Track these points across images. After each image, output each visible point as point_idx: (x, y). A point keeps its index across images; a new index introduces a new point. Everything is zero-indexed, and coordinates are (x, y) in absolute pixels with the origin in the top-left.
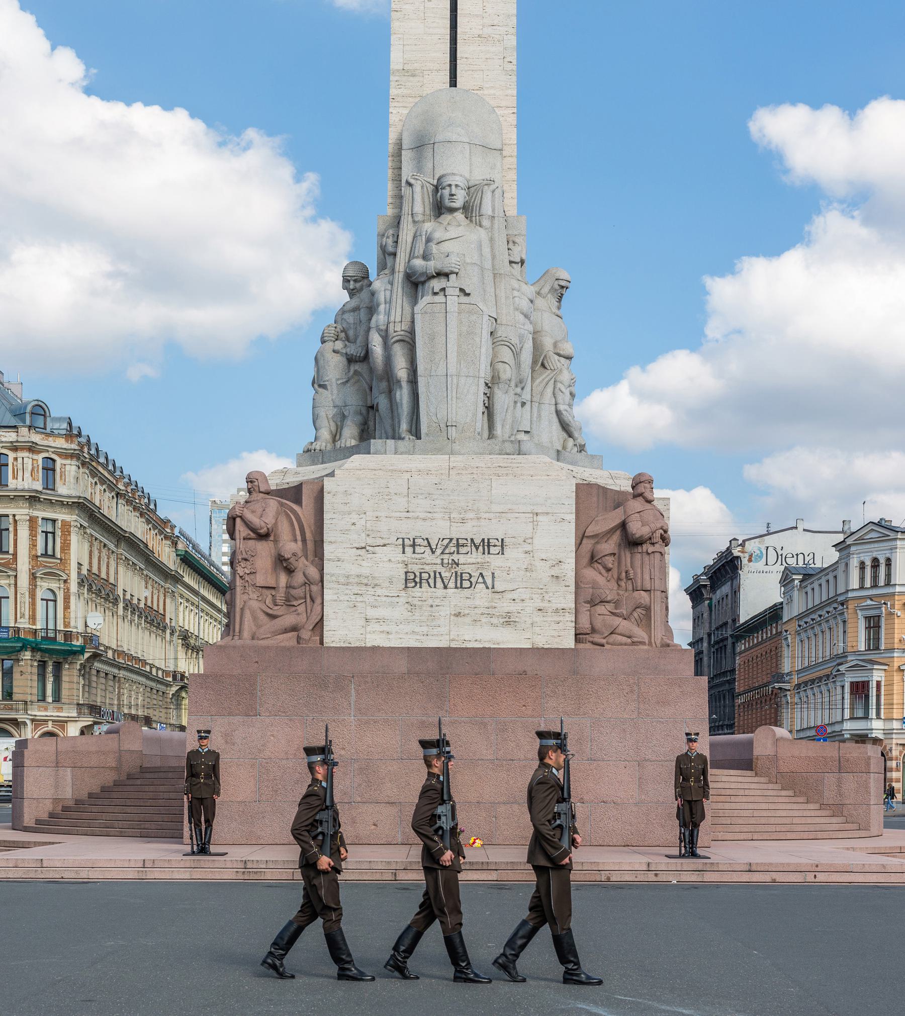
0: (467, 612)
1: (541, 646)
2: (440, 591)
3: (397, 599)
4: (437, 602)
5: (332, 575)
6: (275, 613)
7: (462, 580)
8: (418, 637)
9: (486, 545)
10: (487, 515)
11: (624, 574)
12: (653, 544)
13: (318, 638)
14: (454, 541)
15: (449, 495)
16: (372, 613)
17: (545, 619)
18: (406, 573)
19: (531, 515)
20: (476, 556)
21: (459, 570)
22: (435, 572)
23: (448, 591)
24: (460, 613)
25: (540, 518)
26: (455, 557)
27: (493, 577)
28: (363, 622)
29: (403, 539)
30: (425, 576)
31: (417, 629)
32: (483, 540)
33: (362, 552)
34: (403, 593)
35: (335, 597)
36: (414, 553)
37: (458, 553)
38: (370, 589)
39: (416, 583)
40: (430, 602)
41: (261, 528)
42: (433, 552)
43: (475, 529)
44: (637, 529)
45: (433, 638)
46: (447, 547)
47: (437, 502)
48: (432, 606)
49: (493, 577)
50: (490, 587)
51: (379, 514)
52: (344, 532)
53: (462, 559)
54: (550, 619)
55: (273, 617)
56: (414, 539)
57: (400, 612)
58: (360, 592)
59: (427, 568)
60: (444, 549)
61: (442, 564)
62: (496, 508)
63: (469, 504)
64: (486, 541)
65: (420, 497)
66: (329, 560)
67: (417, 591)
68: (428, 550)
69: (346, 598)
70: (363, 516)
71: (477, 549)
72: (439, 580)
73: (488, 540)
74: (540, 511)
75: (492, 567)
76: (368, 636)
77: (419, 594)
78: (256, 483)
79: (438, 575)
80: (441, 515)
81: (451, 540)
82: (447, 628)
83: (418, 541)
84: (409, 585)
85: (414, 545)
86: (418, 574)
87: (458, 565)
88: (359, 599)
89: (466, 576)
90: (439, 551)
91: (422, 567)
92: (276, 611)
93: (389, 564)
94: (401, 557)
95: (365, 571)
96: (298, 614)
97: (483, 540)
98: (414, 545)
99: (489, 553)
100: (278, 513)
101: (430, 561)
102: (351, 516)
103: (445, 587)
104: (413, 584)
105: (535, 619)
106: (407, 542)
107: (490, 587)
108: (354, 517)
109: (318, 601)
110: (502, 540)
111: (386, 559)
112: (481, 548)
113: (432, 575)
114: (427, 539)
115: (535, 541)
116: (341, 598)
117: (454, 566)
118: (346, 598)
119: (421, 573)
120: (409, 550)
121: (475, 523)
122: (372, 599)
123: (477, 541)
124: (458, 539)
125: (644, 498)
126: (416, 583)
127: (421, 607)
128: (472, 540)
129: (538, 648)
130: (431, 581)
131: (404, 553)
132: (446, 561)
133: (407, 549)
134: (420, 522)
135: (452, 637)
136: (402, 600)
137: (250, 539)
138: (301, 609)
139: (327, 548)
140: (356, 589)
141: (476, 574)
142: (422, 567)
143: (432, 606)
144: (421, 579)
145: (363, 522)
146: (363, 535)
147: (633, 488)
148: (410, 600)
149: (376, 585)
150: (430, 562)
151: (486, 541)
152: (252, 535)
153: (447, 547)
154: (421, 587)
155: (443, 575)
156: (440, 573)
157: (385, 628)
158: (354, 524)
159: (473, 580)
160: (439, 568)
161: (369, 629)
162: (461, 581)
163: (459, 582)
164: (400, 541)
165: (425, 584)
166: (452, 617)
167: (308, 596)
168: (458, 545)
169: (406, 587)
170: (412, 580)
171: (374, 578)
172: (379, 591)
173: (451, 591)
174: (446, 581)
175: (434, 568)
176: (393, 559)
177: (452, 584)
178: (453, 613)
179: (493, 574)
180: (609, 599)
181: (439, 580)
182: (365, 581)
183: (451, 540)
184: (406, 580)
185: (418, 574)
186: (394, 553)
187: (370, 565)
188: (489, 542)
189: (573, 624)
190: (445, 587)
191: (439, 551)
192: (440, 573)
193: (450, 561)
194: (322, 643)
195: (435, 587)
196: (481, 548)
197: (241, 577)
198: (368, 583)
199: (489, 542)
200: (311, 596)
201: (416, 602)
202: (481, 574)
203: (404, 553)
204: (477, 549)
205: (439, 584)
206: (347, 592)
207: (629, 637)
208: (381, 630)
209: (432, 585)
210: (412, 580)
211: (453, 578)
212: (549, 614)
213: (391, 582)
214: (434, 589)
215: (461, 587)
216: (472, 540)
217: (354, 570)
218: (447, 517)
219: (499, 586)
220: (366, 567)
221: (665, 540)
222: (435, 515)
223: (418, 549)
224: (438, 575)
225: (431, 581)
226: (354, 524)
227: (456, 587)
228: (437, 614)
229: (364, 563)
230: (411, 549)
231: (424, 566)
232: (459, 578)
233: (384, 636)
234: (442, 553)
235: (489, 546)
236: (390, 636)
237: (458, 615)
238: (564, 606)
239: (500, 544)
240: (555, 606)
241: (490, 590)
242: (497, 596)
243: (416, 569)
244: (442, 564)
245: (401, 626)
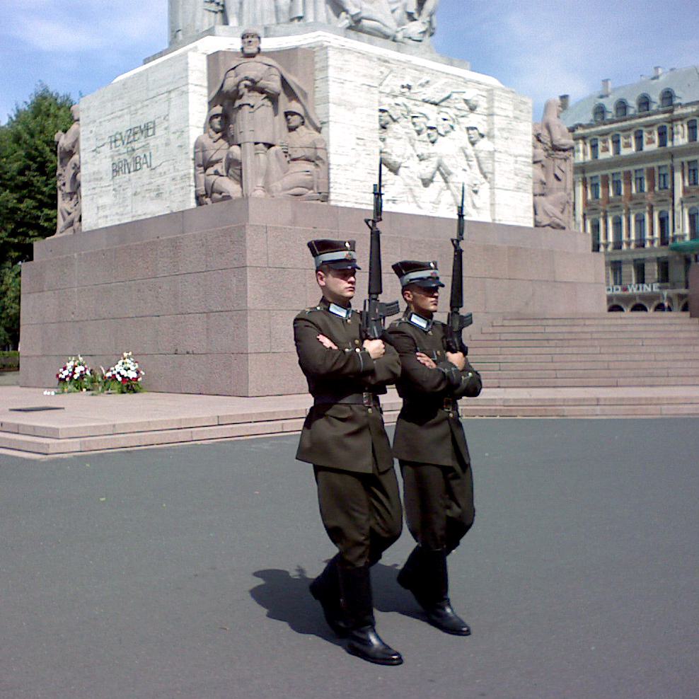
2: (127, 176)
3: (109, 188)
8: (118, 217)
21: (134, 155)
25: (173, 95)
27: (150, 156)
34: (112, 183)
42: (123, 143)
49: (150, 156)
52: (88, 139)
59: (122, 157)
74: (172, 88)
81: (131, 130)
87: (134, 150)
90: (126, 142)
98: (115, 141)
115: (170, 118)
135: (134, 213)
141: (142, 156)
142: (118, 157)
149: (101, 178)
150: (121, 152)
153: (129, 137)
165: (120, 172)
190: (129, 172)
191: (126, 142)
205: (127, 171)
207: (221, 193)
210: (116, 171)
219: (153, 166)
225: (123, 168)
229: (96, 163)
234: (128, 143)
237: (135, 194)
241: (149, 169)
242: (153, 172)
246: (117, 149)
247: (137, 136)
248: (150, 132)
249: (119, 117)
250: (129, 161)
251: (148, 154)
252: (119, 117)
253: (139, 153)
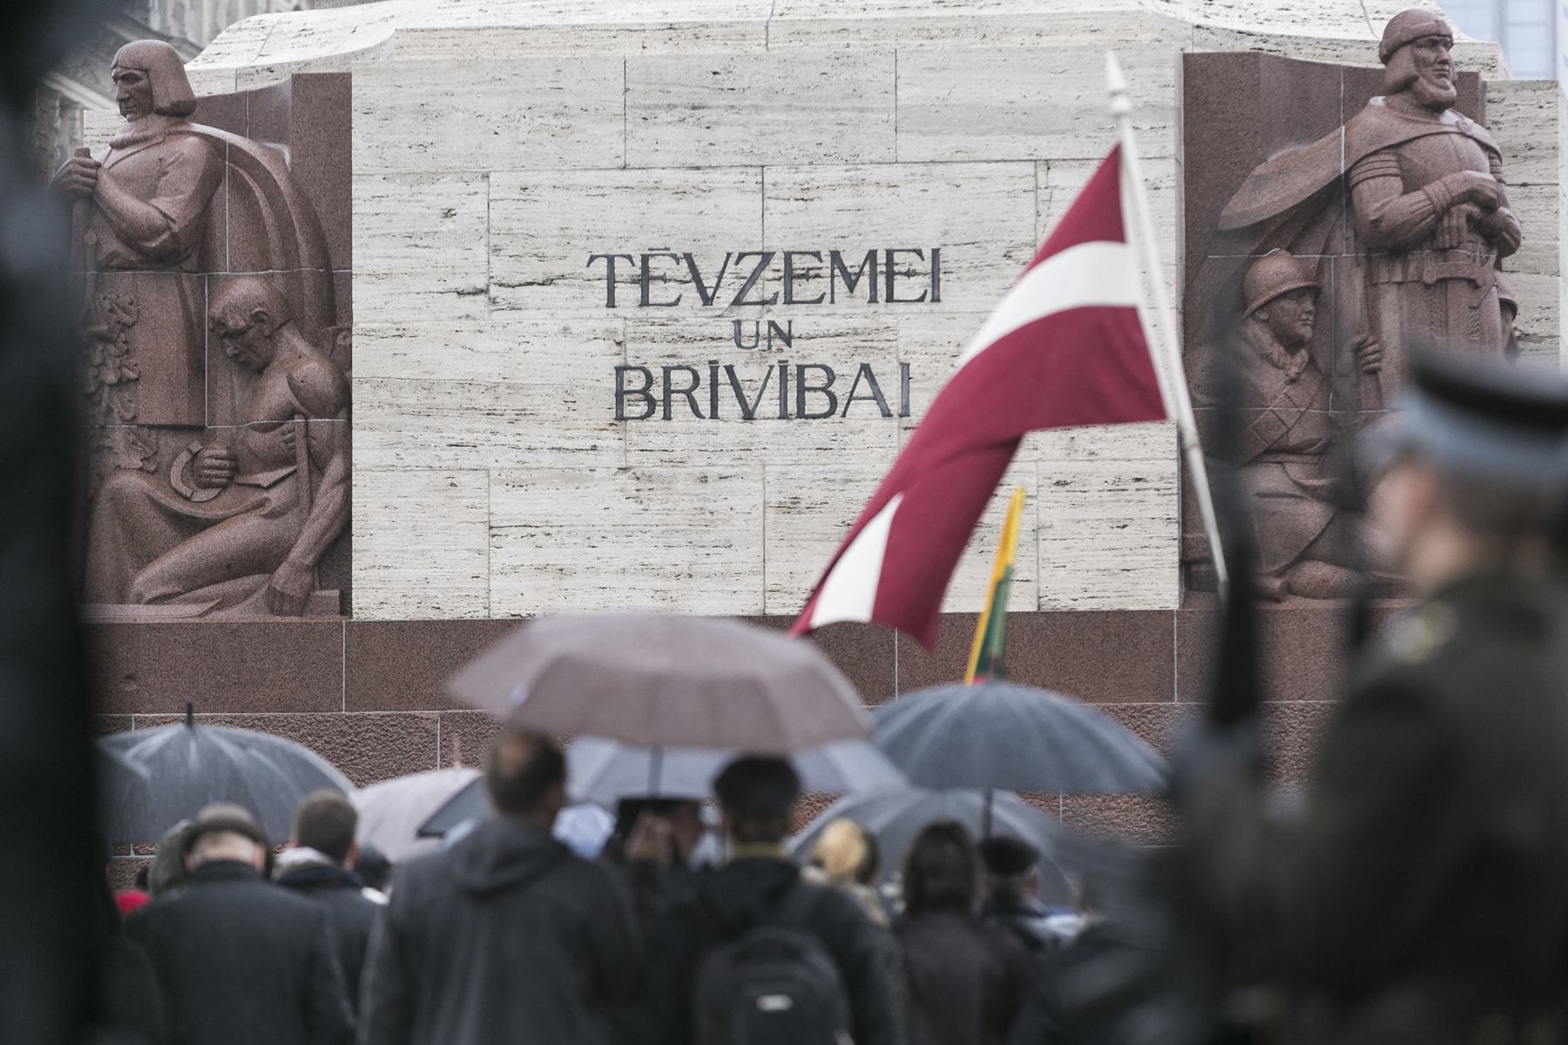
0: (818, 495)
1: (1064, 603)
2: (730, 427)
3: (590, 459)
4: (722, 465)
5: (382, 383)
6: (199, 512)
7: (802, 389)
8: (659, 584)
10: (883, 173)
11: (1347, 357)
12: (1443, 252)
13: (336, 593)
14: (778, 263)
15: (757, 108)
16: (507, 505)
17: (1079, 513)
18: (620, 370)
19: (1030, 168)
20: (851, 310)
22: (714, 366)
23: (757, 426)
24: (796, 500)
26: (780, 314)
27: (906, 378)
28: (479, 538)
29: (611, 260)
30: (681, 379)
31: (658, 557)
32: (872, 255)
33: (478, 304)
34: (610, 440)
35: (389, 457)
36: (644, 303)
37: (789, 301)
38: (502, 426)
39: (652, 403)
40: (699, 465)
41: (155, 232)
42: (707, 301)
43: (846, 219)
44: (1384, 199)
45: (709, 585)
46: (753, 279)
47: (719, 133)
48: (704, 479)
49: (906, 378)
50: (895, 409)
51: (528, 178)
53: (802, 320)
54: (1096, 513)
55: (190, 526)
56: (645, 259)
57: (603, 499)
58: (469, 438)
59: (688, 353)
60: (743, 291)
61: (738, 338)
62: (910, 147)
63: (825, 139)
64: (882, 258)
65: (665, 116)
66: (367, 334)
67: (654, 432)
68: (691, 293)
69: (425, 458)
70: (481, 186)
71: (852, 287)
72: (726, 391)
73: (890, 253)
75: (902, 344)
76: (496, 584)
77: (660, 441)
78: (142, 84)
79: (723, 377)
80: (734, 176)
81: (767, 257)
82: (758, 550)
83: (659, 265)
84: (628, 411)
85: (644, 279)
86: (657, 373)
87: (788, 339)
88: (468, 459)
89: (815, 378)
90: (726, 296)
91: (668, 348)
92: (203, 503)
93: (568, 342)
94: (601, 320)
95: (485, 369)
96: (272, 515)
97: (872, 255)
98: (644, 279)
99: (890, 298)
100: (210, 180)
102: (438, 187)
103: (749, 416)
104: (643, 408)
105: (1048, 516)
106: (622, 267)
107: (895, 409)
108: (449, 191)
109: (335, 468)
110: (936, 252)
111: (552, 326)
112: (864, 282)
113: (705, 374)
114: (688, 257)
116: (409, 460)
117: (778, 343)
118: (425, 458)
119: (667, 371)
120: (628, 294)
121: (846, 199)
122: (508, 459)
123: (853, 260)
124: (788, 256)
125: (1418, 95)
126: (652, 403)
127: (668, 483)
128: (835, 256)
129: (1053, 616)
131: (611, 303)
132: (748, 329)
133: (622, 291)
134: (665, 203)
135: (770, 582)
136: (609, 459)
137: (121, 268)
139: (364, 298)
140: (457, 429)
141: (846, 370)
142: (668, 348)
143: (704, 479)
144: (668, 392)
145: (477, 206)
146: (481, 251)
147: (1385, 59)
148: (633, 459)
149: (522, 413)
150: (698, 331)
151: (882, 258)
153: (753, 279)
154: (667, 417)
155: (741, 374)
156: (730, 370)
157: (552, 554)
158: (448, 214)
159: (840, 389)
160: (727, 353)
161: (499, 559)
163: (792, 396)
164: (601, 267)
165: (680, 407)
166: (771, 514)
167: (302, 453)
168: (789, 276)
169: (621, 418)
171: (514, 388)
172: (533, 434)
173: (766, 427)
174: (750, 395)
175: (710, 351)
176: (576, 327)
177: (769, 406)
178: (774, 500)
179: (905, 367)
180: (1294, 439)
181: (726, 391)
182: (486, 401)
183: (767, 257)
184: (620, 394)
185: (657, 373)
186: (583, 306)
187: (497, 346)
188: (890, 261)
189: (1175, 530)
190: (749, 416)
191: (726, 296)
192: (730, 370)
193: (764, 329)
195: (714, 416)
196: (864, 282)
198: (501, 404)
199: (890, 261)
200: (310, 455)
201: (650, 464)
202: (865, 368)
203: (611, 303)
204: (852, 287)
205: (729, 404)
206: (427, 437)
208: (541, 562)
209: (705, 408)
210: (641, 395)
211: (774, 382)
212: (1093, 496)
213: (570, 403)
214: (709, 423)
215: (801, 414)
216: (835, 256)
217: (452, 366)
218: (752, 178)
220: (483, 351)
221: (1498, 237)
222: (714, 176)
223: (657, 292)
224: (723, 377)
225: (702, 396)
226: (448, 214)
227: (784, 415)
228: (721, 506)
229: (483, 343)
230: (636, 292)
231: (679, 347)
232: (792, 384)
233: (547, 581)
234: (738, 302)
235: (890, 276)
236: (568, 582)
237: (791, 506)
238: (1143, 469)
239: (927, 266)
240: (1110, 470)
241: (894, 423)
243: (653, 356)
244: (738, 338)
245: (605, 549)
246: (652, 312)
247: (802, 290)
248: (902, 287)
249: (681, 193)
252: (681, 193)
253: (821, 352)
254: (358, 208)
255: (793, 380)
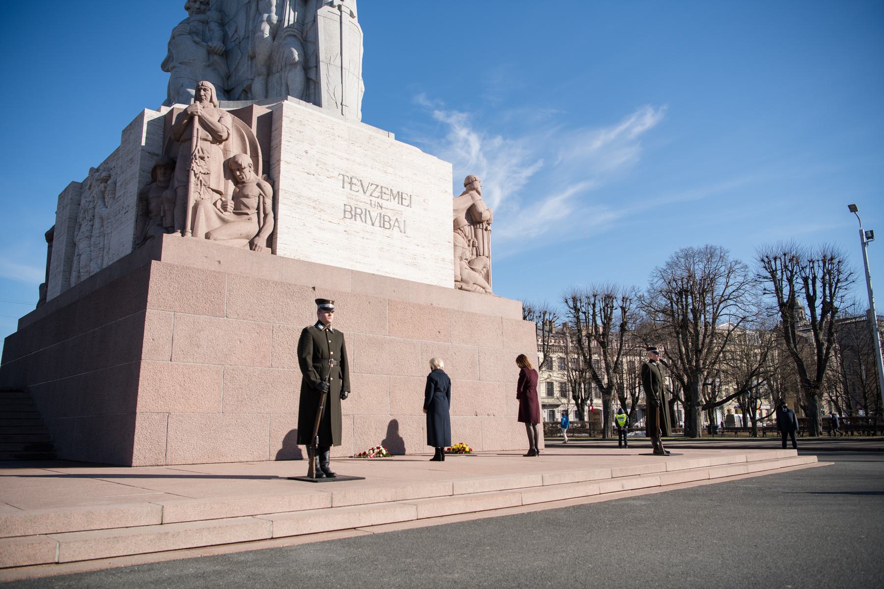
2: (369, 226)
9: (400, 196)
14: (379, 189)
20: (394, 204)
21: (383, 212)
26: (379, 200)
30: (359, 211)
42: (365, 193)
53: (385, 204)
59: (361, 205)
83: (354, 181)
85: (351, 183)
89: (387, 219)
90: (368, 193)
101: (362, 200)
120: (347, 186)
123: (395, 192)
130: (363, 216)
132: (373, 203)
138: (255, 218)
141: (394, 219)
144: (356, 214)
152: (210, 138)
159: (392, 223)
160: (369, 208)
162: (384, 222)
170: (352, 213)
173: (377, 228)
174: (374, 219)
177: (377, 223)
182: (313, 204)
184: (345, 211)
194: (274, 252)
197: (195, 175)
225: (363, 216)
243: (353, 203)
247: (385, 197)
248: (406, 202)
250: (374, 215)
251: (401, 220)
254: (283, 142)
255: (382, 217)
